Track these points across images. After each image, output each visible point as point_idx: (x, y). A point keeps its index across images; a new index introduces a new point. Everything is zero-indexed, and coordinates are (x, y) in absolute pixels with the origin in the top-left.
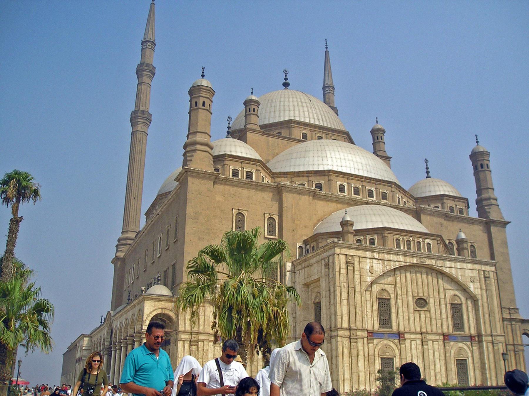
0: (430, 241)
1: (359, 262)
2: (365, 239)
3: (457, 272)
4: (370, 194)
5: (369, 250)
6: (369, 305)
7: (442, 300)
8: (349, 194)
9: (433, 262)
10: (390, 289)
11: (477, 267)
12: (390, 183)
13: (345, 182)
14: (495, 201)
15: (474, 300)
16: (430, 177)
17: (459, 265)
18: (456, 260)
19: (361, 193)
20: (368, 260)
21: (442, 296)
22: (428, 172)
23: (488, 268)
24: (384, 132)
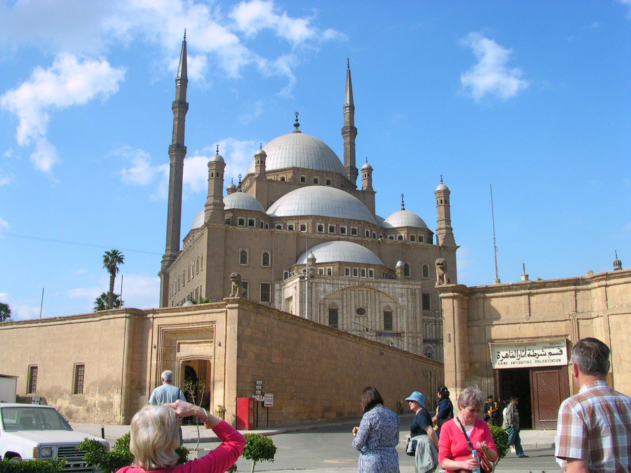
0: (372, 269)
1: (316, 286)
4: (343, 231)
5: (323, 278)
7: (377, 309)
10: (338, 302)
11: (405, 286)
12: (360, 221)
13: (323, 223)
15: (402, 308)
16: (404, 209)
17: (391, 286)
18: (388, 283)
20: (322, 285)
21: (378, 306)
23: (415, 287)
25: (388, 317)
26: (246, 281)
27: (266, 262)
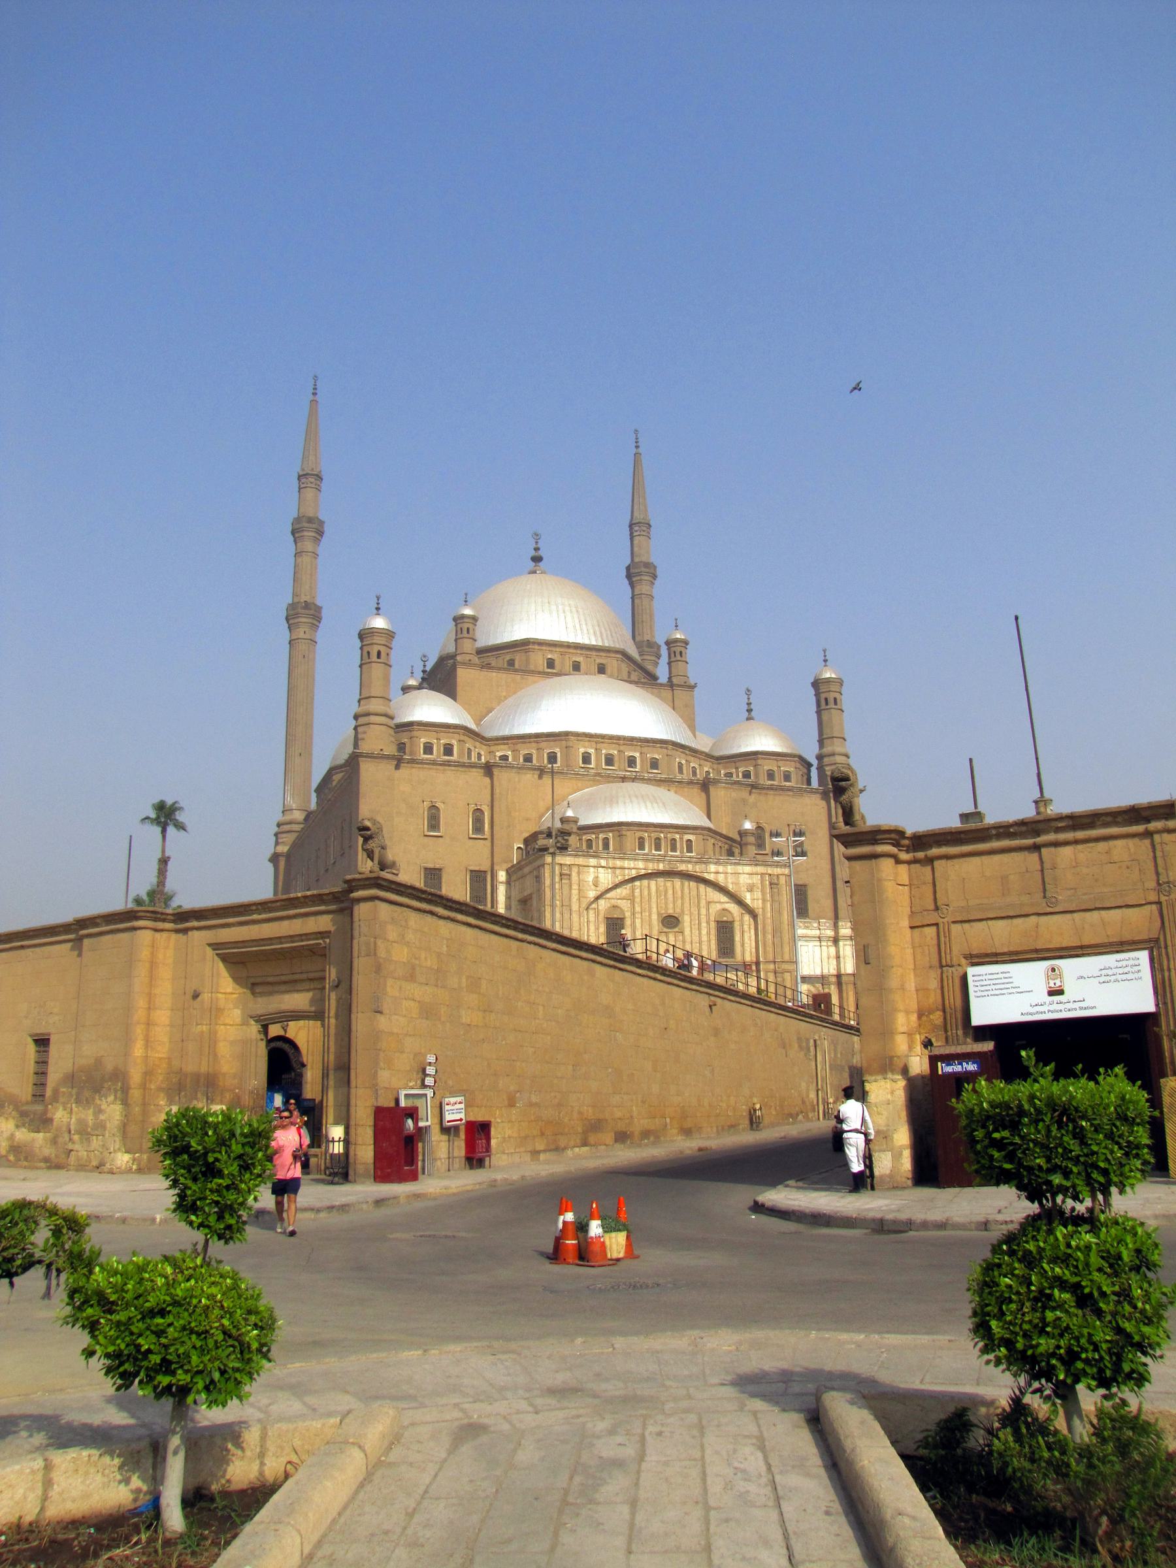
2: (597, 838)
3: (726, 878)
5: (594, 857)
6: (592, 928)
8: (597, 765)
9: (690, 867)
10: (625, 905)
11: (760, 869)
14: (844, 758)
17: (730, 869)
19: (616, 764)
20: (592, 869)
21: (703, 911)
22: (749, 711)
23: (778, 871)
24: (686, 643)
25: (725, 931)
26: (437, 866)
27: (478, 828)
